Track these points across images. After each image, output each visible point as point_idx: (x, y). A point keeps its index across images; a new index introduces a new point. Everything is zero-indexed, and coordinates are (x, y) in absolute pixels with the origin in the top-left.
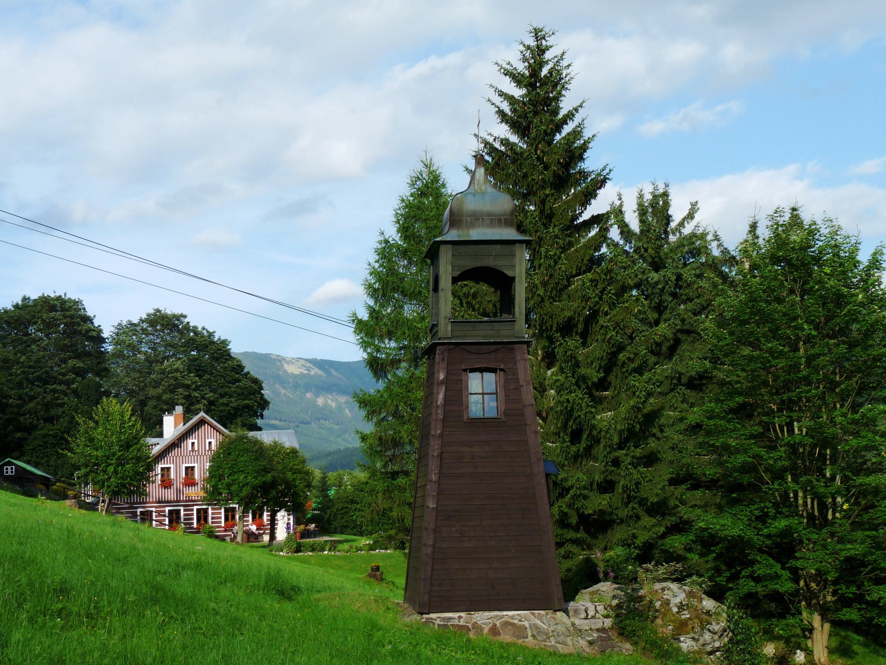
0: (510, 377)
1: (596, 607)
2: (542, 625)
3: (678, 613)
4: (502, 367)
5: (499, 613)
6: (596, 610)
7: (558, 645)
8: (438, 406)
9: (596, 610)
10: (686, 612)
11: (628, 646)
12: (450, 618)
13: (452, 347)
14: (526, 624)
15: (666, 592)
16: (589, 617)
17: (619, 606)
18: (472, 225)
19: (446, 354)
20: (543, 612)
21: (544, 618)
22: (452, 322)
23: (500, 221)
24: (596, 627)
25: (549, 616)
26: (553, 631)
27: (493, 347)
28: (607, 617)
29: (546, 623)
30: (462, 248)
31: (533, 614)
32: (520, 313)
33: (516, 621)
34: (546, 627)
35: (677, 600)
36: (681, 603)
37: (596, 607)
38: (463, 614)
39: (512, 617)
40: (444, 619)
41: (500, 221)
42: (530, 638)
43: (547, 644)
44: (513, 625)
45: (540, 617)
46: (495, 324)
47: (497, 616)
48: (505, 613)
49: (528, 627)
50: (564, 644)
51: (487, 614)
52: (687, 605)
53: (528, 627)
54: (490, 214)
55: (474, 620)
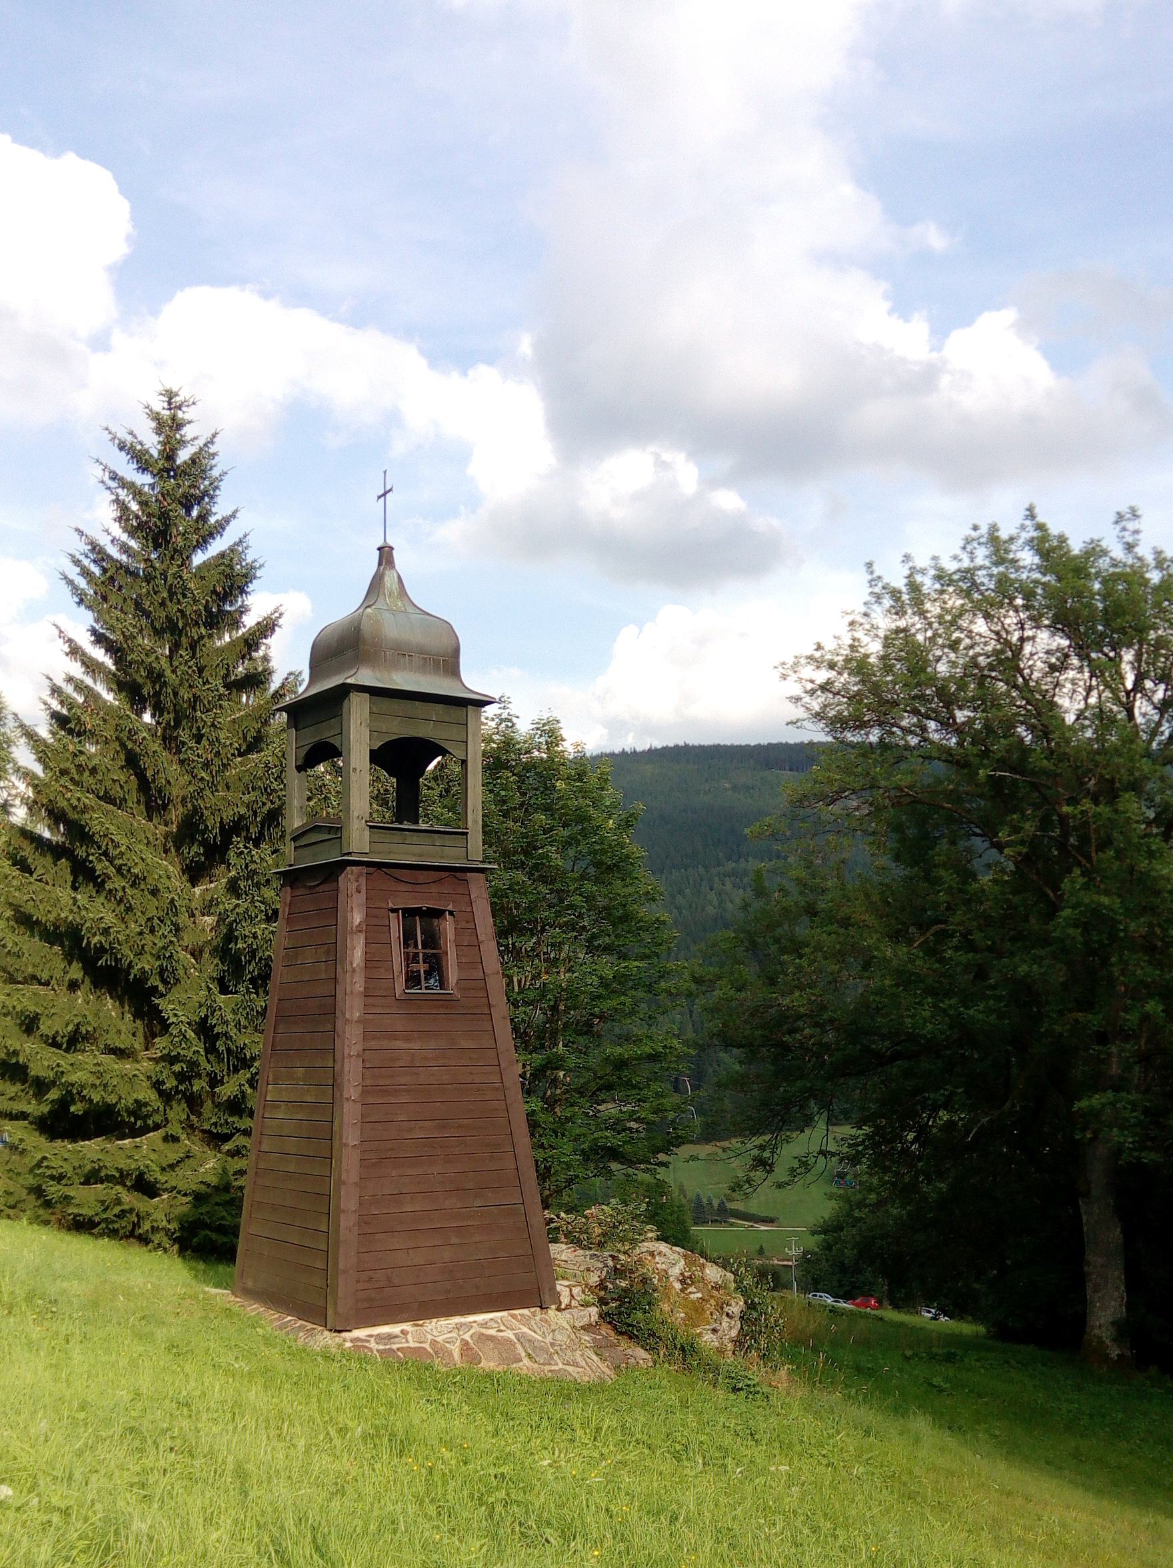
0: (463, 925)
1: (571, 1290)
2: (533, 1334)
3: (682, 1290)
4: (450, 908)
5: (458, 1319)
6: (572, 1296)
7: (568, 1368)
8: (354, 971)
9: (572, 1296)
10: (692, 1289)
11: (641, 1353)
12: (390, 1337)
13: (371, 870)
14: (509, 1334)
15: (657, 1259)
16: (563, 1306)
17: (602, 1286)
18: (394, 665)
19: (363, 881)
20: (525, 1312)
21: (533, 1322)
22: (371, 827)
23: (436, 663)
24: (581, 1324)
25: (538, 1318)
26: (552, 1344)
27: (434, 875)
28: (586, 1305)
29: (538, 1331)
30: (386, 704)
31: (514, 1316)
32: (475, 821)
33: (492, 1332)
34: (540, 1338)
35: (675, 1271)
36: (682, 1274)
37: (571, 1290)
38: (406, 1326)
39: (484, 1325)
40: (379, 1338)
41: (436, 663)
42: (526, 1361)
43: (553, 1368)
44: (491, 1338)
45: (524, 1321)
46: (436, 836)
47: (462, 1324)
48: (471, 1318)
49: (513, 1338)
50: (576, 1365)
51: (443, 1322)
52: (690, 1277)
53: (513, 1338)
54: (422, 651)
55: (429, 1337)
